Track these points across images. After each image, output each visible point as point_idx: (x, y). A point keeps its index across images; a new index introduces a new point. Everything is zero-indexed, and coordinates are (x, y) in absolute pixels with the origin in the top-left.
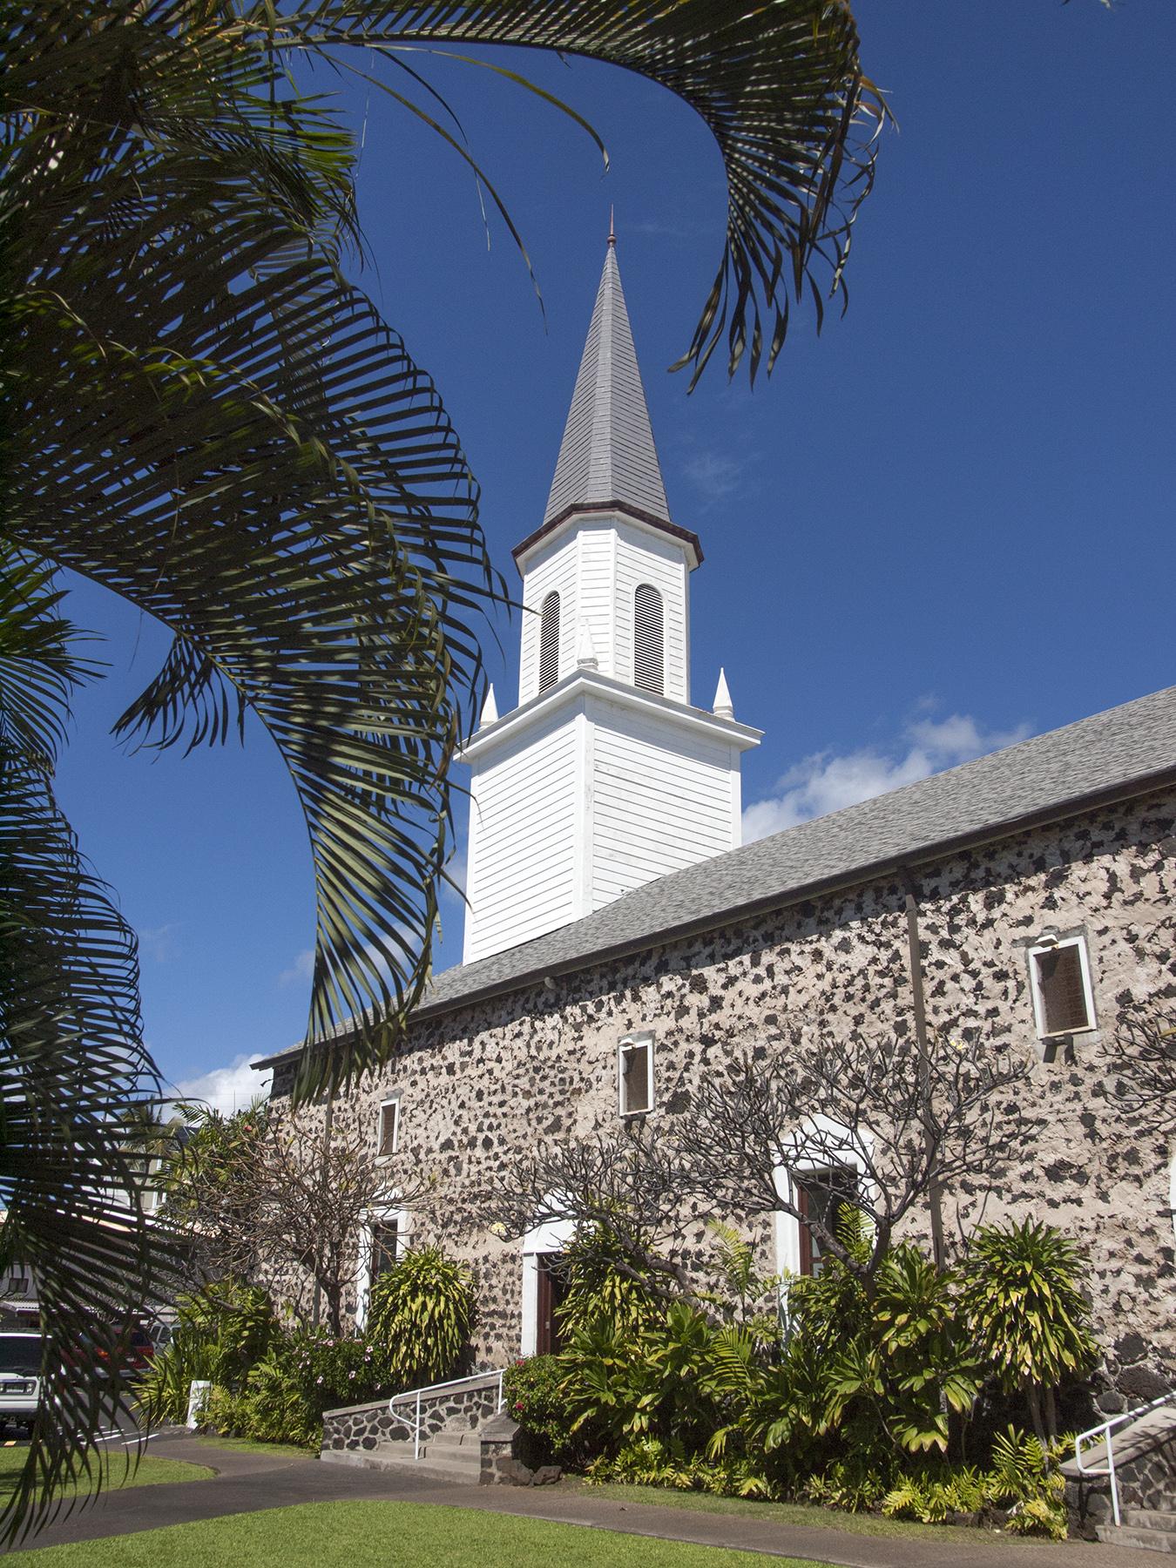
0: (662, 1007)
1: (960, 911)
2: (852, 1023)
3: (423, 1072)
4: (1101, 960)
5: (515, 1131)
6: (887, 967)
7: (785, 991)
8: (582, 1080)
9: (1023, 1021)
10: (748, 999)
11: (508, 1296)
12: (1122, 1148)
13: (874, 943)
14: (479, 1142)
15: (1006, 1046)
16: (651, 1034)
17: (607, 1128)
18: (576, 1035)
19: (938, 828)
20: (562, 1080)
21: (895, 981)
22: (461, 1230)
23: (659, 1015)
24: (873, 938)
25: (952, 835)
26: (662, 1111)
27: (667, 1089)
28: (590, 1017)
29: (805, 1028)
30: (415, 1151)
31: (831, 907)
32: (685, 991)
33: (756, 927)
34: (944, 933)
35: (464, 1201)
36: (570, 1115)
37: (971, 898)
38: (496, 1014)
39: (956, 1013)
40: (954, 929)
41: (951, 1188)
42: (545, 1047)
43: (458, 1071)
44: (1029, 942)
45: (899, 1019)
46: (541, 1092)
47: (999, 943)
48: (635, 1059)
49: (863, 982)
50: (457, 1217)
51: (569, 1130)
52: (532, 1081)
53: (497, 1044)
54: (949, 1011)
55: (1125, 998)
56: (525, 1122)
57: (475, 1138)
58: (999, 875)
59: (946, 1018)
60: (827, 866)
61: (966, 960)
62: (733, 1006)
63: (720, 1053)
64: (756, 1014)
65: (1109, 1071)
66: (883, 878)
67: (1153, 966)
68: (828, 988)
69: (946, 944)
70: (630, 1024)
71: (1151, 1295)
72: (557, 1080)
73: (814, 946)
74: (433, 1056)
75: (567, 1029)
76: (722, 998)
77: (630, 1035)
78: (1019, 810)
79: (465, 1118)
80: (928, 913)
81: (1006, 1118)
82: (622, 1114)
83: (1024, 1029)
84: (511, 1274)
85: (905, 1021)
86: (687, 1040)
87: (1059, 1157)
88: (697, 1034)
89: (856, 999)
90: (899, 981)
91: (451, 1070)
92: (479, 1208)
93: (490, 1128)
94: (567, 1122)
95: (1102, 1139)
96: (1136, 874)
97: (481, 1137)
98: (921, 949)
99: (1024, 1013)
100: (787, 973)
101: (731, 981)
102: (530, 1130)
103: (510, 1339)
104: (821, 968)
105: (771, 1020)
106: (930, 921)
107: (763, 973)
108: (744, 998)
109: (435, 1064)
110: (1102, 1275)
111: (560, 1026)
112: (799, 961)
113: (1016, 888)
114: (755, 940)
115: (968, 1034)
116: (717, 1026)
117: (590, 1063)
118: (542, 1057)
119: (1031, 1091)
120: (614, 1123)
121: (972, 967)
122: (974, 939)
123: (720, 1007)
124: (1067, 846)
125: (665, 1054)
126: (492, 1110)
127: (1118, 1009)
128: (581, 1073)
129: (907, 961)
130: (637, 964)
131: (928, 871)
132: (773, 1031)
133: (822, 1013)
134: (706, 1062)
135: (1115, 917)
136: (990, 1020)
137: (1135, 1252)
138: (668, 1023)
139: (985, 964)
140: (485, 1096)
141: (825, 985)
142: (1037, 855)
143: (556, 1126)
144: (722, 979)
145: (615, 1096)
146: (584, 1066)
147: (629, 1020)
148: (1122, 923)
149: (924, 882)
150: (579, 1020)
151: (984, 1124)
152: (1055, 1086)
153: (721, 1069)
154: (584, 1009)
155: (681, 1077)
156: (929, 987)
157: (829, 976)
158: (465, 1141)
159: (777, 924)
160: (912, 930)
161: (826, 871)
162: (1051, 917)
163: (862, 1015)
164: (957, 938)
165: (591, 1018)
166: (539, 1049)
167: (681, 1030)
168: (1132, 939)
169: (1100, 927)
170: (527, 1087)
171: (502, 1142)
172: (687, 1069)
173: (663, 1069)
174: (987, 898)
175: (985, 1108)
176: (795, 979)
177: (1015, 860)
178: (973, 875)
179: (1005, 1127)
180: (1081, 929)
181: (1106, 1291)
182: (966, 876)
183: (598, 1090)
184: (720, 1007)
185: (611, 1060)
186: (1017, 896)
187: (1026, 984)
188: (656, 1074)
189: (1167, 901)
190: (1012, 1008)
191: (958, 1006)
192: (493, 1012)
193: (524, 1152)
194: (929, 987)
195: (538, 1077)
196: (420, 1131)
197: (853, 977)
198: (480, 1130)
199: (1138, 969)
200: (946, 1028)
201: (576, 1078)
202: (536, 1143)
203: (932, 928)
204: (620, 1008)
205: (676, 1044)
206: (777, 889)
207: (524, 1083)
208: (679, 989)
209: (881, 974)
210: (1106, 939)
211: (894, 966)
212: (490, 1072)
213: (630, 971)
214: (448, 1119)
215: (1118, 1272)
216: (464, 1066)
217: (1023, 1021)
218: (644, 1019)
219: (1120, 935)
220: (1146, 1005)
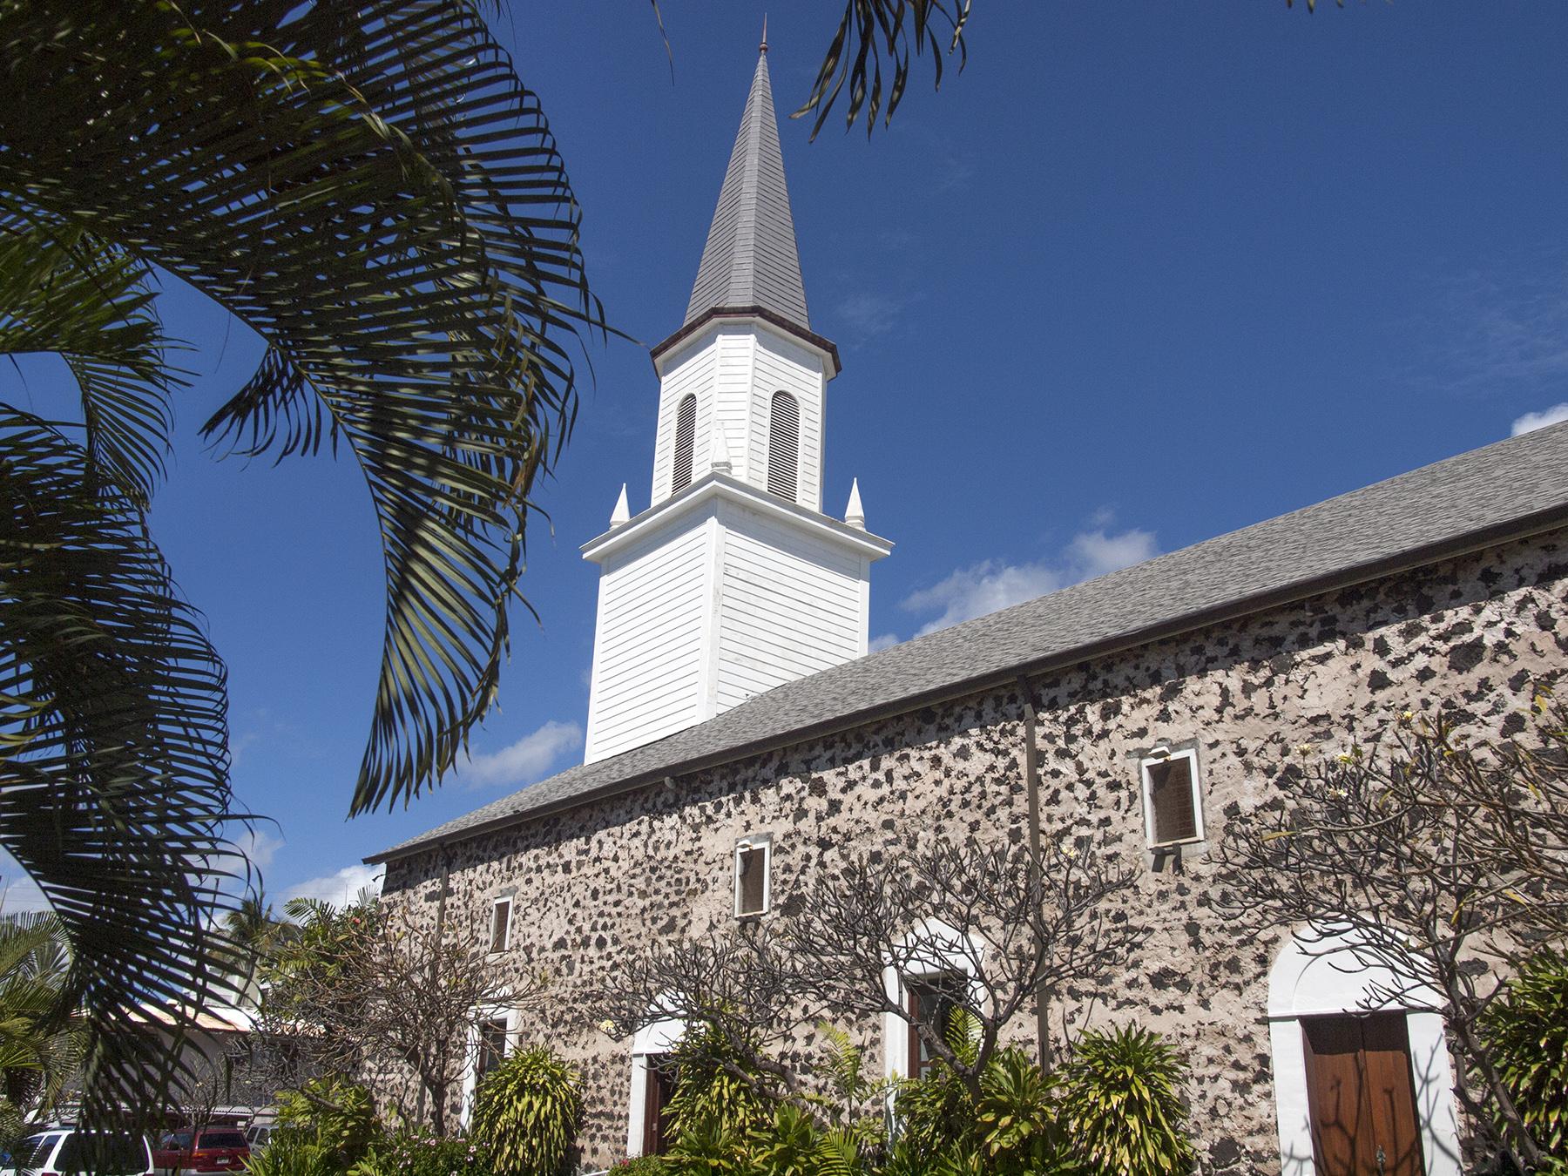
0: (781, 810)
1: (1077, 722)
2: (967, 830)
3: (539, 870)
4: (1211, 773)
5: (629, 931)
6: (1004, 775)
7: (903, 796)
8: (698, 880)
9: (1134, 831)
10: (866, 803)
11: (616, 1097)
12: (1224, 957)
13: (992, 751)
14: (593, 942)
15: (1116, 855)
16: (769, 837)
17: (722, 930)
18: (694, 835)
19: (1059, 640)
20: (679, 880)
21: (1012, 788)
22: (571, 1030)
23: (778, 818)
24: (991, 745)
25: (1072, 646)
26: (777, 913)
27: (783, 891)
28: (709, 818)
29: (922, 834)
30: (528, 950)
31: (951, 715)
32: (804, 794)
33: (876, 732)
34: (1061, 743)
35: (575, 1000)
36: (685, 915)
37: (1088, 709)
38: (616, 812)
39: (1069, 822)
40: (1071, 739)
41: (1058, 994)
42: (662, 846)
43: (574, 870)
44: (1142, 753)
45: (1014, 826)
46: (657, 892)
47: (1113, 753)
48: (752, 862)
49: (980, 789)
50: (568, 1017)
51: (683, 931)
52: (648, 881)
53: (615, 843)
54: (1063, 820)
55: (1232, 810)
56: (639, 922)
57: (589, 938)
58: (1116, 687)
59: (1060, 826)
61: (1081, 769)
62: (851, 810)
63: (836, 856)
64: (873, 818)
65: (1214, 881)
66: (1004, 686)
67: (1260, 779)
68: (945, 795)
69: (1062, 754)
70: (748, 826)
71: (1246, 1100)
72: (673, 881)
73: (933, 752)
74: (549, 854)
75: (685, 829)
76: (840, 802)
77: (747, 837)
78: (1138, 624)
79: (579, 917)
80: (1046, 723)
82: (737, 916)
83: (1134, 838)
84: (620, 1075)
86: (805, 843)
87: (1163, 964)
88: (815, 837)
89: (973, 806)
91: (567, 868)
93: (605, 927)
94: (681, 923)
95: (1205, 948)
96: (1248, 689)
97: (595, 936)
98: (1037, 758)
99: (1135, 823)
100: (906, 778)
101: (851, 785)
102: (644, 931)
103: (616, 1140)
104: (939, 774)
105: (888, 825)
106: (1048, 731)
107: (882, 778)
108: (862, 802)
109: (551, 862)
110: (1200, 1081)
111: (678, 826)
112: (917, 767)
114: (876, 745)
115: (1080, 843)
116: (835, 830)
117: (707, 864)
118: (658, 857)
119: (1139, 900)
120: (728, 924)
121: (1087, 776)
122: (1089, 749)
123: (839, 811)
124: (1182, 660)
125: (782, 857)
126: (607, 909)
127: (1225, 821)
128: (697, 874)
129: (1023, 770)
130: (757, 766)
131: (1048, 681)
132: (890, 835)
133: (938, 818)
134: (822, 864)
135: (1226, 731)
136: (1102, 829)
137: (1232, 1059)
138: (786, 825)
139: (1099, 774)
140: (600, 895)
141: (942, 791)
142: (1153, 667)
143: (670, 927)
144: (841, 783)
145: (731, 898)
146: (700, 867)
147: (748, 822)
148: (1232, 736)
149: (1044, 692)
150: (697, 821)
151: (1093, 931)
152: (1162, 895)
153: (837, 872)
154: (703, 809)
155: (797, 880)
156: (1044, 795)
157: (946, 783)
158: (579, 940)
159: (898, 729)
160: (1029, 739)
161: (948, 678)
162: (1164, 730)
163: (977, 822)
164: (1074, 748)
165: (710, 819)
166: (656, 849)
167: (798, 833)
168: (1241, 752)
169: (1211, 741)
170: (643, 887)
171: (616, 941)
173: (779, 871)
174: (1104, 709)
175: (1094, 916)
176: (914, 785)
177: (1131, 672)
178: (1091, 687)
179: (1113, 934)
180: (1192, 742)
181: (1203, 1096)
182: (1084, 687)
183: (713, 891)
184: (839, 811)
185: (728, 861)
186: (1133, 708)
187: (1139, 795)
188: (772, 876)
189: (1276, 716)
190: (1124, 818)
191: (1072, 814)
192: (612, 810)
193: (637, 952)
194: (1044, 795)
195: (654, 877)
196: (534, 929)
197: (971, 784)
198: (594, 929)
199: (1246, 782)
200: (1060, 836)
201: (693, 879)
202: (650, 943)
203: (1050, 738)
204: (739, 809)
205: (793, 846)
206: (900, 695)
207: (640, 883)
208: (798, 792)
209: (998, 781)
210: (1217, 752)
211: (1012, 775)
212: (607, 871)
213: (750, 773)
215: (1216, 1078)
216: (580, 865)
217: (1134, 831)
218: (762, 821)
219: (1230, 749)
220: (1252, 818)
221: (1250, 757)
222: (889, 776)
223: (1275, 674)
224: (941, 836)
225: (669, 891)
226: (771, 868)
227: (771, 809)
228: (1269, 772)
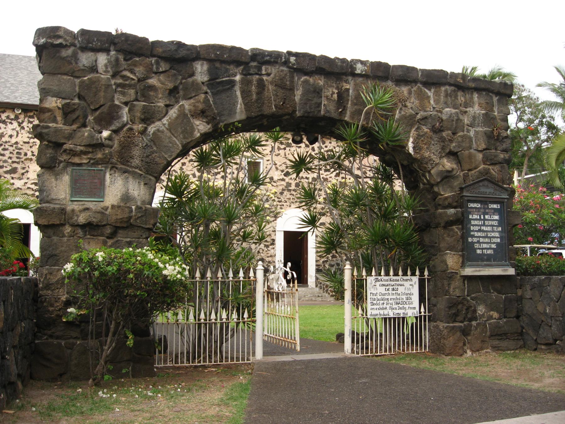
67: (279, 173)
221: (277, 166)
223: (287, 147)
228: (282, 171)
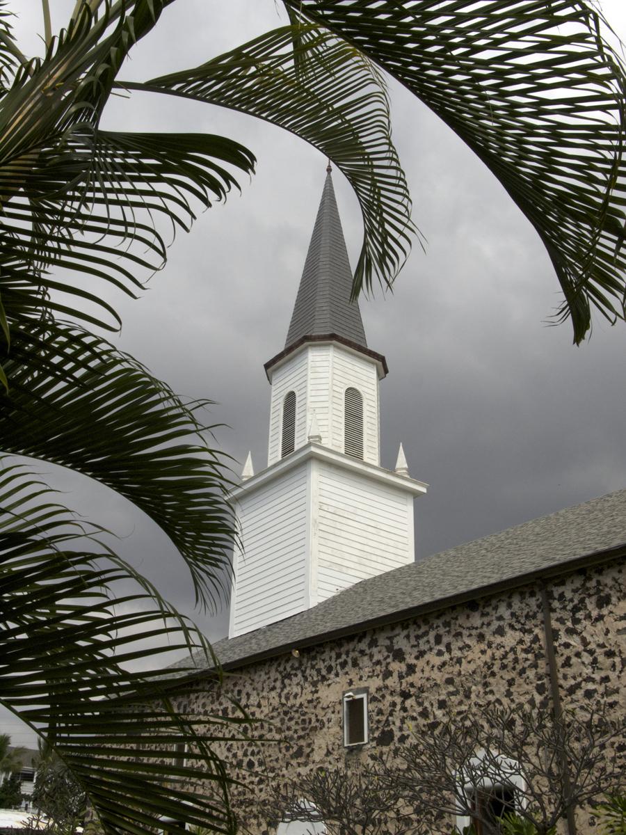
0: (374, 671)
2: (506, 685)
5: (270, 756)
6: (530, 646)
7: (459, 661)
8: (317, 720)
10: (433, 666)
13: (521, 630)
14: (245, 764)
15: (616, 703)
16: (366, 690)
19: (560, 552)
20: (304, 721)
23: (371, 677)
25: (573, 557)
26: (374, 744)
27: (378, 728)
29: (474, 688)
32: (389, 660)
33: (438, 617)
34: (569, 624)
36: (309, 745)
37: (587, 601)
38: (258, 673)
39: (579, 679)
41: (581, 803)
42: (291, 697)
43: (230, 713)
45: (539, 682)
46: (289, 729)
48: (355, 706)
49: (514, 656)
51: (308, 756)
52: (282, 721)
53: (258, 695)
54: (574, 678)
56: (277, 749)
57: (242, 761)
58: (606, 585)
59: (572, 682)
60: (485, 577)
61: (585, 642)
62: (423, 671)
63: (414, 703)
64: (438, 676)
66: (526, 586)
68: (489, 660)
69: (570, 632)
70: (351, 683)
72: (300, 721)
73: (478, 631)
74: (212, 702)
75: (307, 685)
76: (415, 666)
77: (350, 690)
79: (235, 746)
80: (558, 610)
81: (618, 754)
82: (346, 745)
85: (543, 684)
86: (391, 694)
88: (398, 689)
89: (509, 668)
90: (538, 656)
92: (245, 811)
93: (253, 754)
94: (307, 750)
97: (246, 760)
98: (553, 635)
100: (460, 649)
101: (421, 654)
102: (281, 756)
104: (483, 646)
105: (450, 681)
106: (559, 616)
107: (444, 649)
108: (431, 666)
111: (302, 683)
112: (468, 642)
113: (619, 594)
114: (438, 627)
115: (589, 694)
116: (412, 685)
117: (323, 709)
118: (289, 704)
120: (340, 751)
121: (589, 647)
122: (590, 628)
123: (414, 672)
125: (376, 704)
128: (316, 716)
130: (356, 641)
132: (451, 689)
133: (485, 677)
134: (404, 709)
136: (603, 685)
139: (599, 645)
140: (249, 731)
141: (487, 658)
143: (299, 753)
145: (341, 733)
146: (319, 711)
147: (351, 680)
149: (554, 589)
150: (315, 679)
153: (415, 714)
154: (319, 671)
155: (387, 720)
156: (560, 661)
157: (489, 652)
158: (235, 763)
161: (485, 580)
164: (579, 627)
165: (324, 678)
166: (287, 698)
167: (386, 687)
170: (279, 725)
171: (261, 764)
172: (391, 714)
174: (598, 600)
176: (466, 653)
179: (618, 760)
182: (583, 585)
183: (328, 728)
184: (414, 672)
185: (338, 707)
186: (619, 599)
188: (370, 717)
190: (619, 677)
191: (581, 674)
192: (256, 672)
193: (276, 771)
194: (560, 661)
195: (286, 718)
198: (245, 755)
200: (572, 690)
201: (314, 720)
202: (285, 765)
203: (561, 621)
205: (383, 697)
206: (452, 592)
208: (385, 659)
209: (526, 651)
211: (536, 646)
213: (351, 646)
214: (223, 747)
218: (361, 679)
222: (449, 649)
224: (488, 689)
225: (297, 727)
226: (368, 712)
227: (366, 671)
